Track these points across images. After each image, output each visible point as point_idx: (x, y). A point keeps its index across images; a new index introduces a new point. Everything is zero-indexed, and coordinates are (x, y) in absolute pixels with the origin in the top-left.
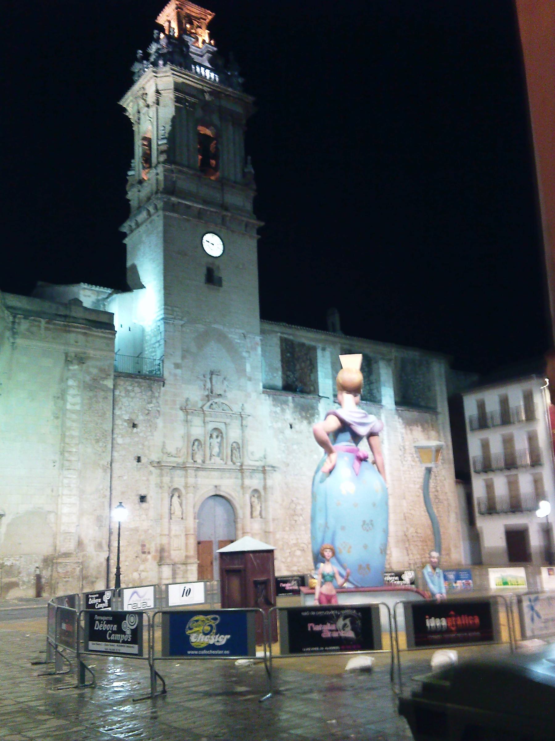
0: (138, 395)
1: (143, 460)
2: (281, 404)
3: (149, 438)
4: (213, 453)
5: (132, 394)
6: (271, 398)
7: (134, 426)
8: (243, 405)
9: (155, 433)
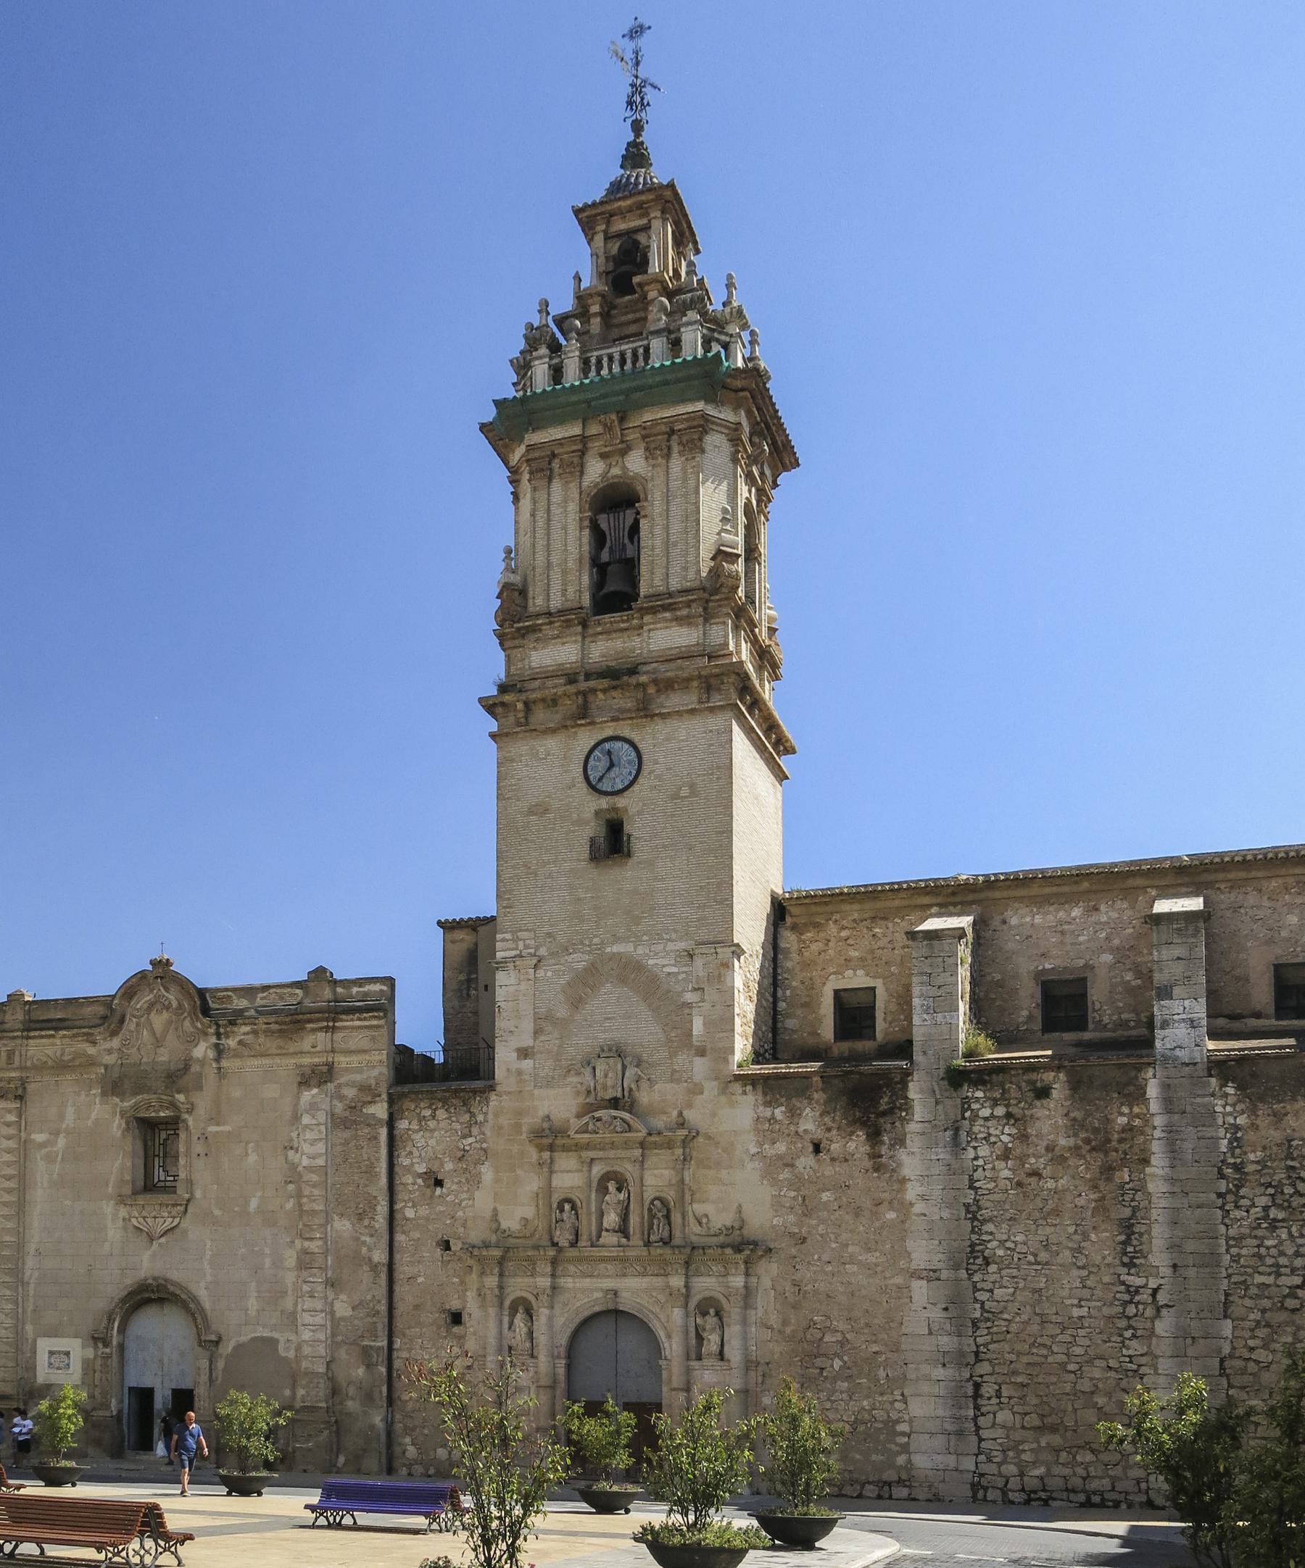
0: (442, 1124)
1: (456, 1246)
2: (789, 1099)
3: (464, 1204)
4: (605, 1225)
5: (432, 1124)
6: (760, 1088)
7: (439, 1183)
8: (680, 1114)
9: (477, 1193)
